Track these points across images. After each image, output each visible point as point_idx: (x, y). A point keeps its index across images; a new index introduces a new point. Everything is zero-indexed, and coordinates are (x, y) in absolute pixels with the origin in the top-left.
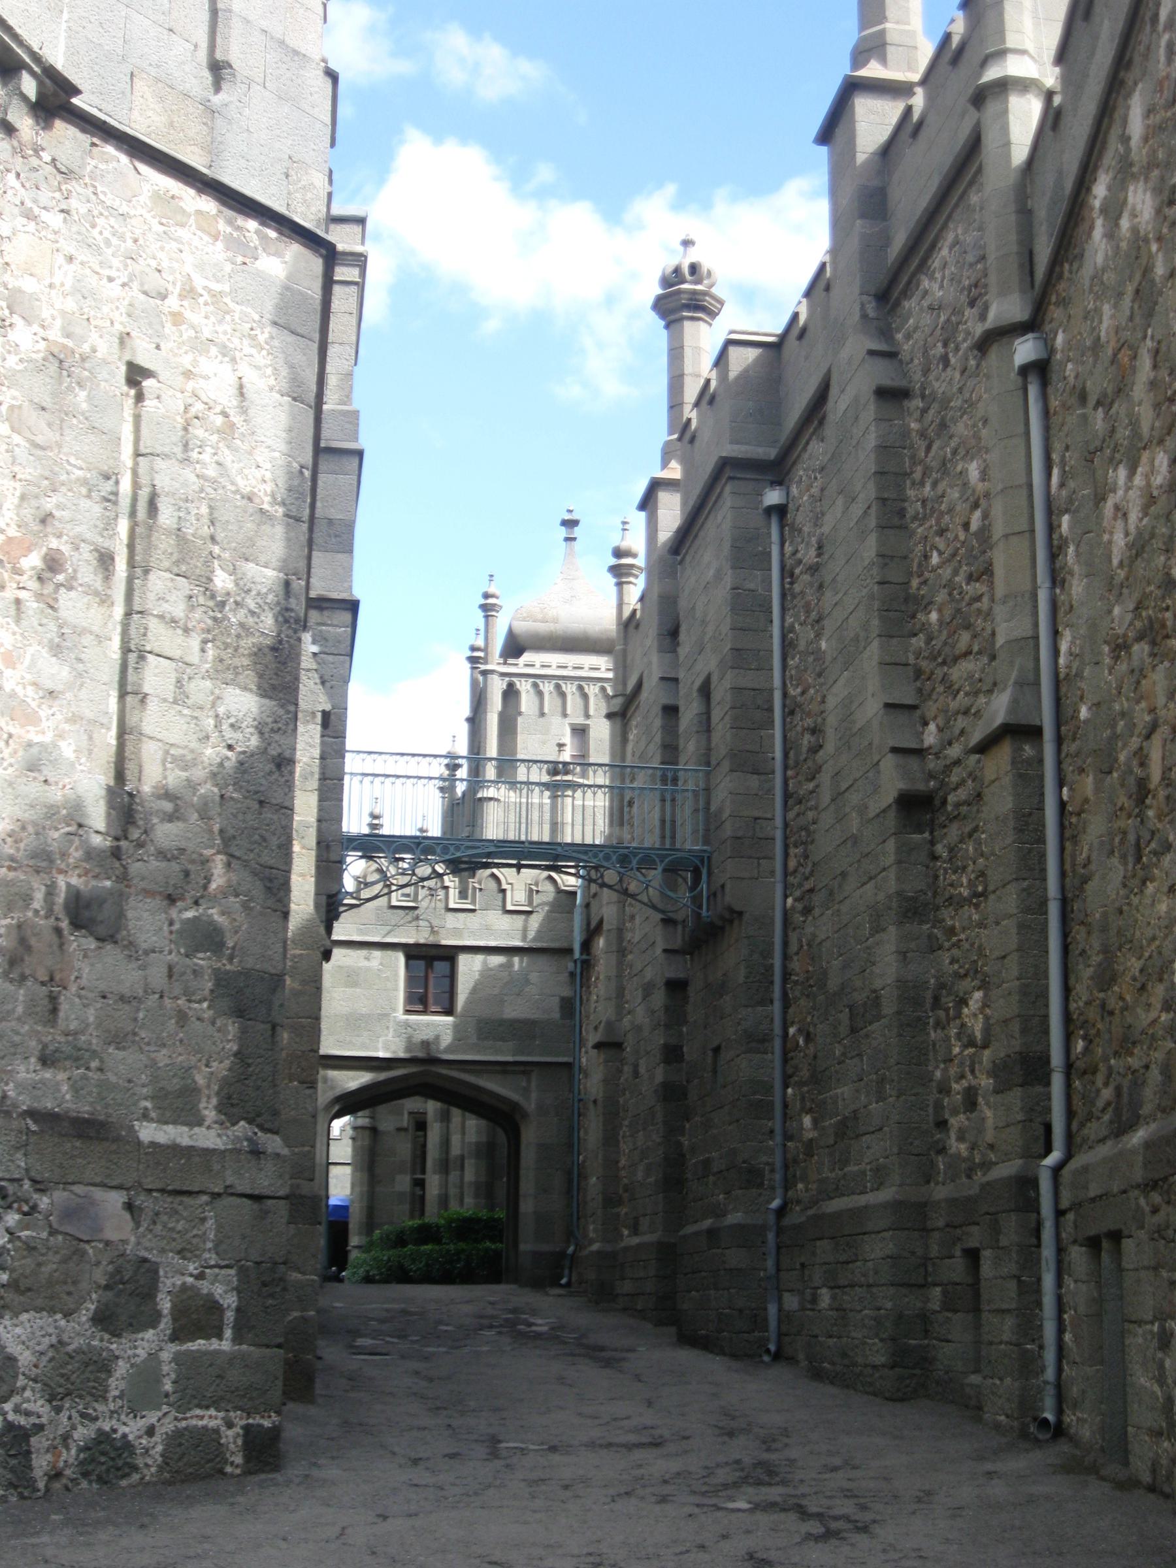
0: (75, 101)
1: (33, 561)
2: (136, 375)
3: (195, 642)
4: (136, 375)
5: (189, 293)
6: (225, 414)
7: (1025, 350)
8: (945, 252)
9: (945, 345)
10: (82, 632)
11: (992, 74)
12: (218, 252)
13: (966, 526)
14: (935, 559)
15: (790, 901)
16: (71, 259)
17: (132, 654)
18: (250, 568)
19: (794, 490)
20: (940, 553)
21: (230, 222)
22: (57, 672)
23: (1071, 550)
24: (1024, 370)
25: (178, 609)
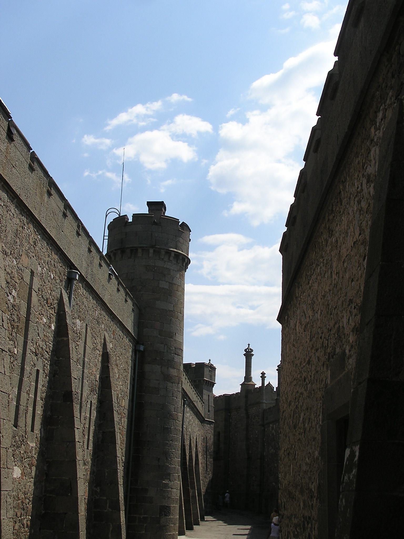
7: (263, 428)
12: (209, 425)
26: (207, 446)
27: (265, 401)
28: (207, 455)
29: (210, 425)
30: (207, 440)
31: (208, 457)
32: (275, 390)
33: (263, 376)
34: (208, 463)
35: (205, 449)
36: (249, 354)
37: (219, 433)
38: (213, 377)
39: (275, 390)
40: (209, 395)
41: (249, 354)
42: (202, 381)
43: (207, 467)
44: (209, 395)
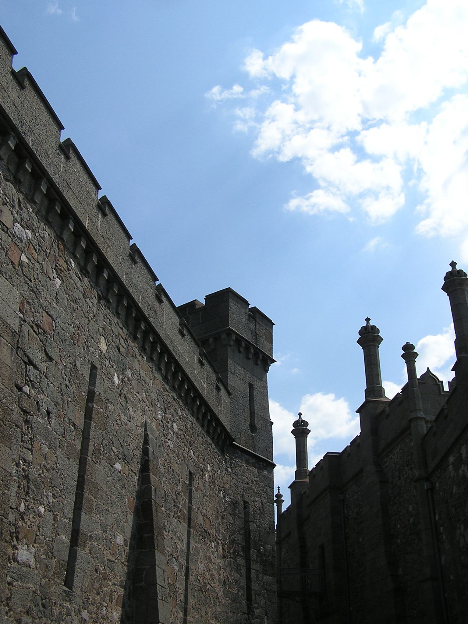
0: (234, 442)
1: (232, 551)
2: (245, 502)
3: (259, 565)
4: (245, 502)
5: (252, 482)
6: (260, 510)
8: (398, 450)
9: (399, 473)
10: (240, 566)
11: (413, 415)
12: (256, 471)
13: (409, 521)
14: (399, 526)
15: (351, 608)
16: (233, 478)
17: (248, 570)
18: (266, 546)
19: (347, 496)
20: (400, 525)
21: (258, 464)
22: (237, 576)
23: (444, 536)
24: (427, 490)
25: (255, 558)
26: (247, 533)
27: (421, 414)
28: (248, 560)
29: (259, 468)
30: (247, 514)
31: (256, 567)
32: (446, 388)
33: (409, 354)
34: (255, 586)
35: (239, 538)
36: (369, 338)
37: (322, 548)
38: (263, 340)
39: (446, 388)
40: (251, 386)
41: (369, 338)
42: (224, 336)
43: (249, 598)
44: (251, 386)
